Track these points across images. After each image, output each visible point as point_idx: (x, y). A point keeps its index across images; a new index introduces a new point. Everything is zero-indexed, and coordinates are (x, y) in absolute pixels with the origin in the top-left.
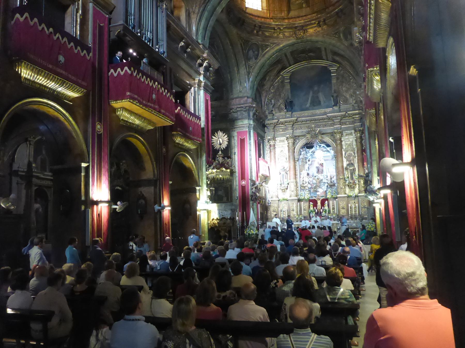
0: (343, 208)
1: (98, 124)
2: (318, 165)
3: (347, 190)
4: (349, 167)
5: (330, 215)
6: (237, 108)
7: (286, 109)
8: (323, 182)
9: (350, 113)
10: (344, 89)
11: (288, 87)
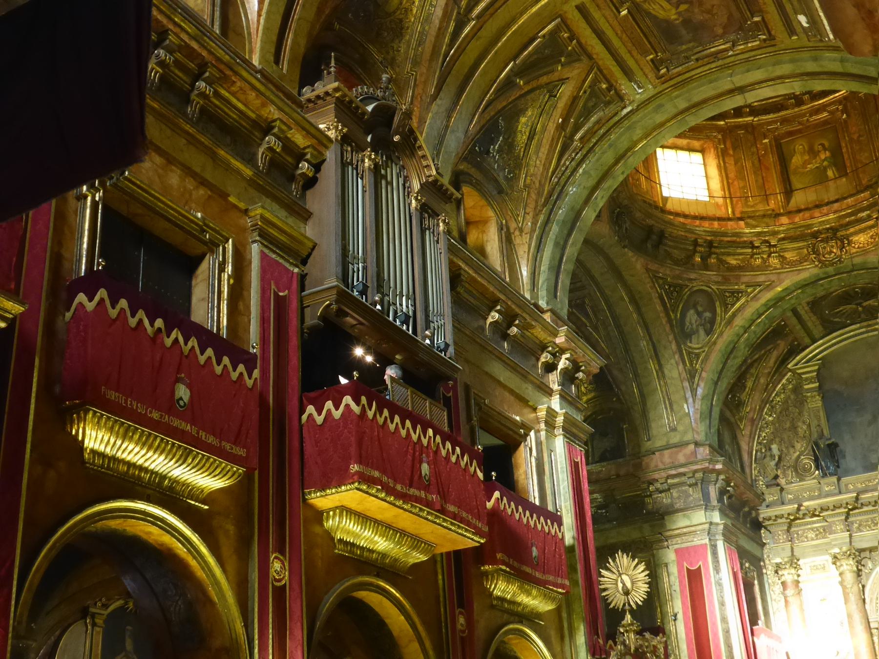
1: (276, 558)
6: (668, 478)
7: (817, 468)
11: (816, 403)
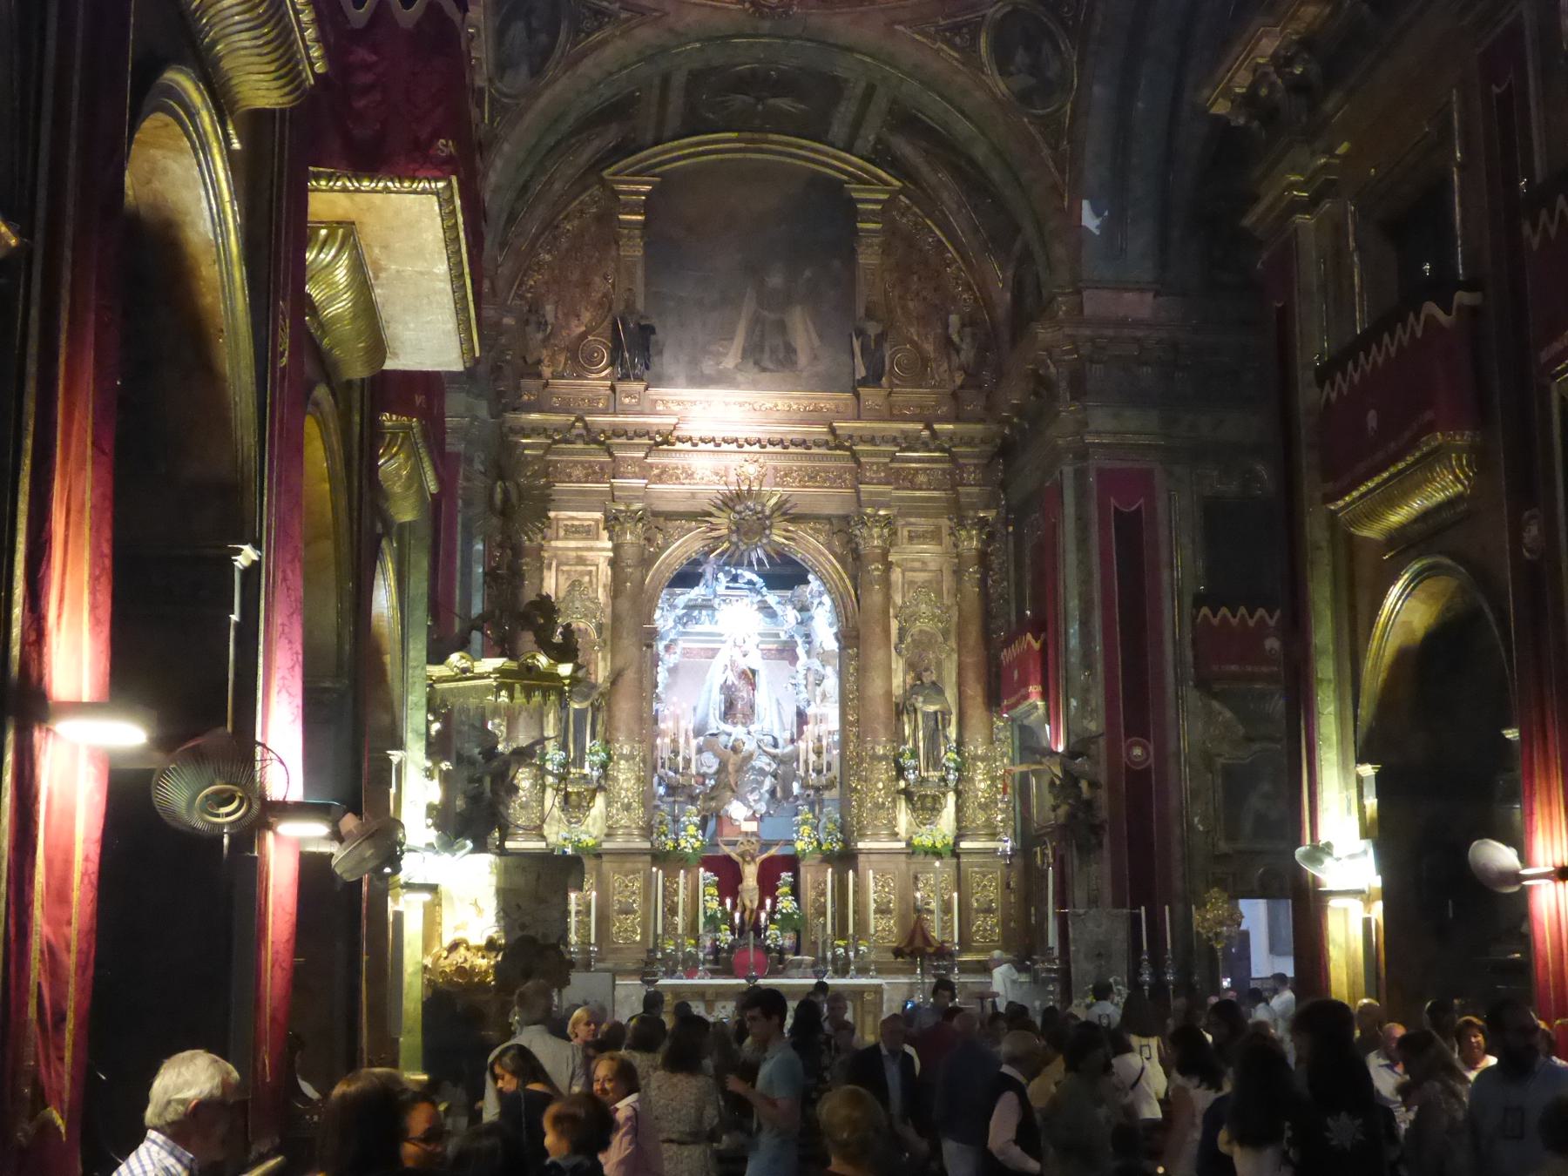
0: (883, 907)
2: (732, 678)
3: (904, 818)
4: (925, 702)
5: (842, 943)
7: (612, 363)
8: (753, 768)
9: (943, 432)
10: (911, 305)
11: (634, 250)
